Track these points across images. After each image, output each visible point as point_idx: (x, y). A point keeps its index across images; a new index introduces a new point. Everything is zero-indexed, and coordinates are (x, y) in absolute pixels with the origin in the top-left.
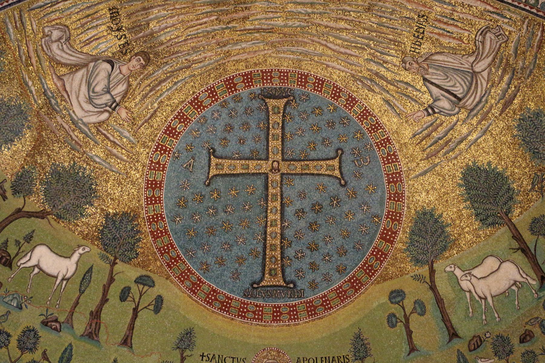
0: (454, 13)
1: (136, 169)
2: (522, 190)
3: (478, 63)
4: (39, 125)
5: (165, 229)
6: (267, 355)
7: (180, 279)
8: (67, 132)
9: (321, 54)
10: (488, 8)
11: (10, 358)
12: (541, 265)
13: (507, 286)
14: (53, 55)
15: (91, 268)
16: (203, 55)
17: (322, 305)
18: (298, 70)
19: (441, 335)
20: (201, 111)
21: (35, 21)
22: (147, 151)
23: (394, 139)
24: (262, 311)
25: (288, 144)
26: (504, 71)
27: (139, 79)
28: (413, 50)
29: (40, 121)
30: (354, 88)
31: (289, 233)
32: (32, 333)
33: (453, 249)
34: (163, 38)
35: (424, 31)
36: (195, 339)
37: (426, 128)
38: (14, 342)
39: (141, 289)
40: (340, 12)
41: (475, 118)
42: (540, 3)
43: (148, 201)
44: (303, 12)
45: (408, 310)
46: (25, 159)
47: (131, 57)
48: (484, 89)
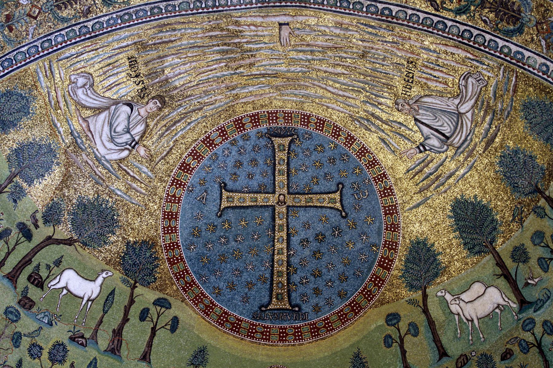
0: (439, 59)
1: (154, 202)
2: (504, 221)
3: (462, 105)
4: (67, 162)
5: (180, 256)
7: (194, 302)
8: (91, 168)
9: (322, 96)
10: (469, 55)
12: (520, 289)
13: (491, 309)
14: (79, 100)
15: (114, 290)
16: (214, 98)
17: (325, 327)
18: (301, 111)
19: (431, 354)
20: (213, 148)
21: (63, 70)
22: (164, 185)
23: (390, 175)
24: (269, 332)
25: (293, 179)
26: (486, 113)
27: (156, 120)
28: (404, 93)
29: (68, 158)
30: (352, 128)
31: (295, 260)
33: (444, 276)
34: (177, 84)
35: (413, 76)
36: (208, 356)
37: (419, 164)
38: (45, 355)
39: (158, 311)
40: (337, 58)
41: (462, 155)
42: (513, 52)
43: (165, 231)
44: (304, 58)
45: (403, 331)
46: (54, 192)
47: (149, 100)
48: (469, 129)
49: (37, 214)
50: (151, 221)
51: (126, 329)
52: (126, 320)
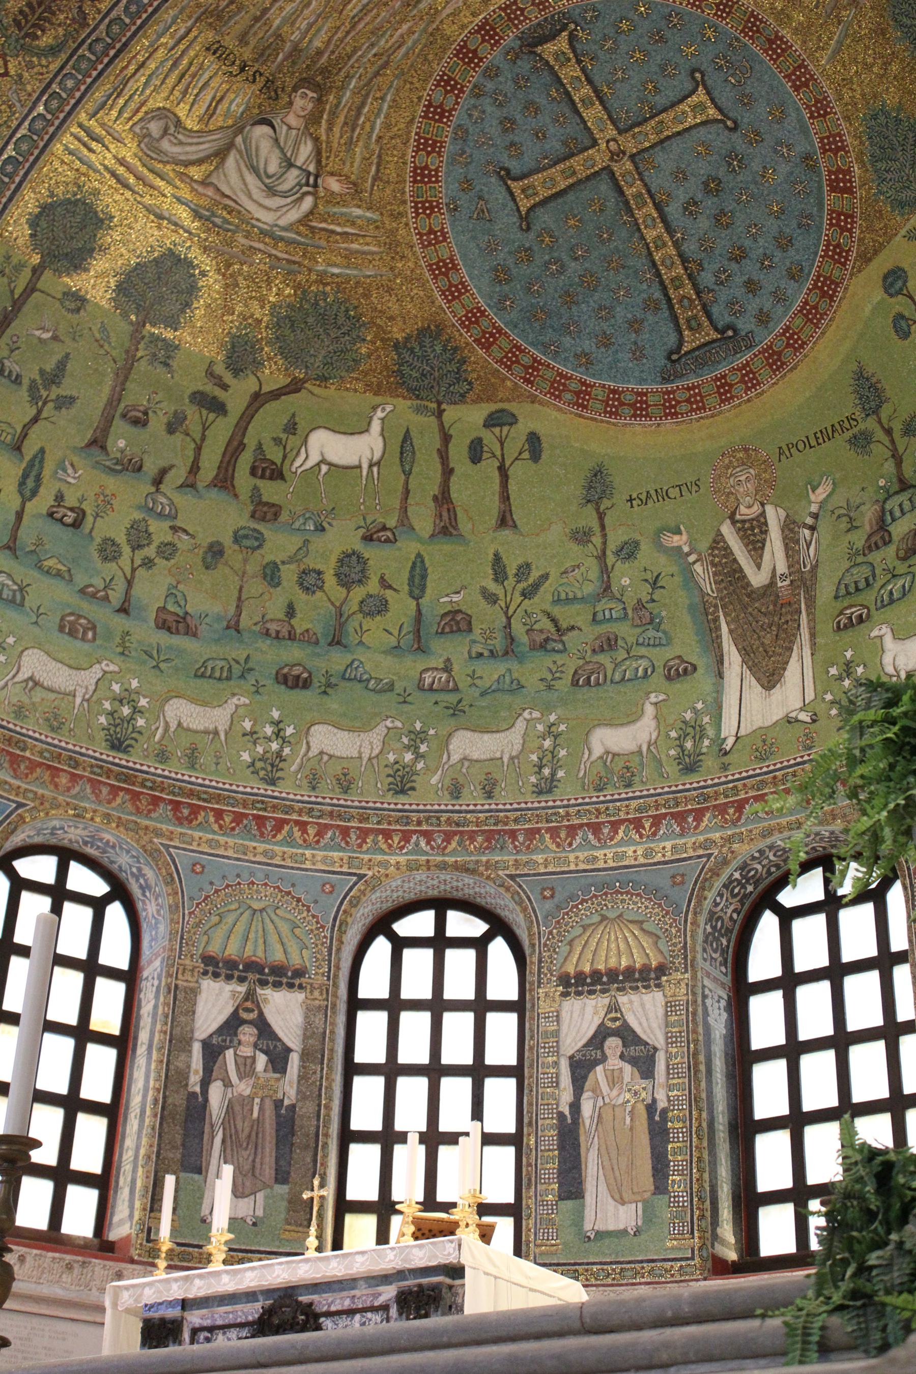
1: (403, 257)
5: (494, 327)
6: (731, 462)
7: (553, 394)
11: (332, 604)
15: (408, 431)
17: (788, 345)
24: (700, 394)
25: (614, 104)
31: (690, 247)
32: (354, 558)
34: (317, 44)
36: (611, 479)
38: (330, 580)
39: (498, 434)
43: (446, 297)
47: (290, 96)
49: (215, 368)
50: (415, 291)
51: (454, 488)
52: (448, 472)
